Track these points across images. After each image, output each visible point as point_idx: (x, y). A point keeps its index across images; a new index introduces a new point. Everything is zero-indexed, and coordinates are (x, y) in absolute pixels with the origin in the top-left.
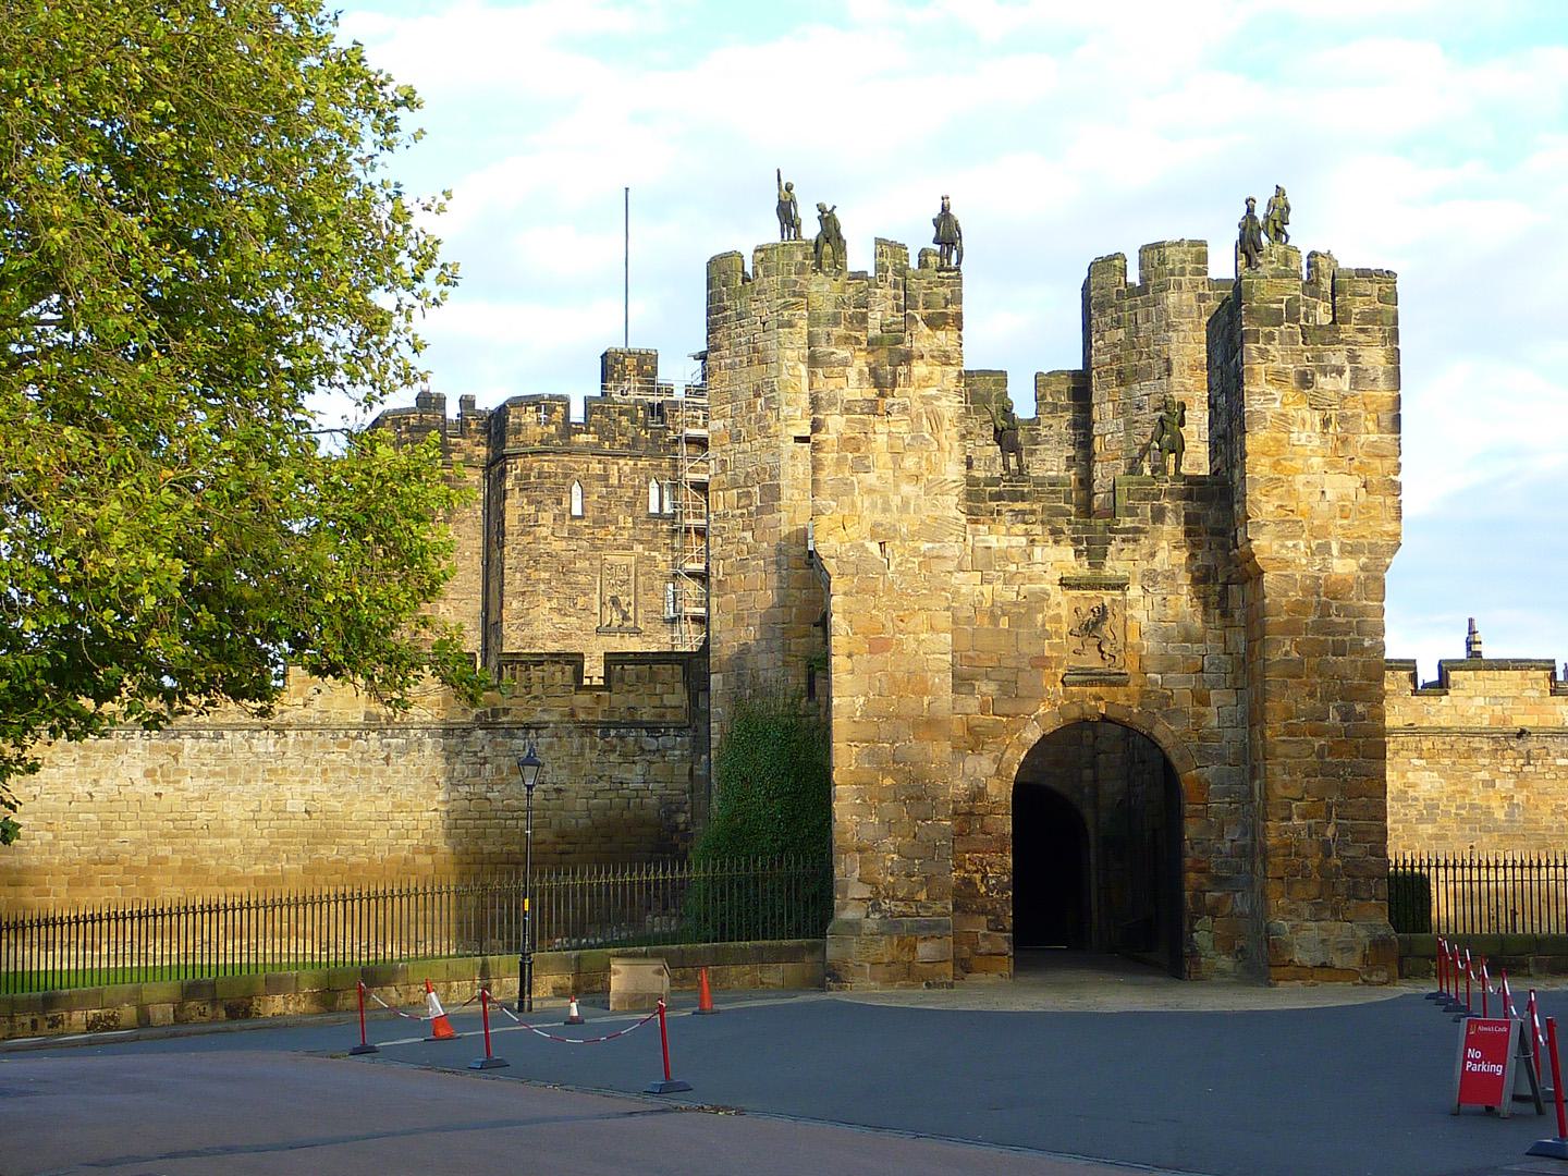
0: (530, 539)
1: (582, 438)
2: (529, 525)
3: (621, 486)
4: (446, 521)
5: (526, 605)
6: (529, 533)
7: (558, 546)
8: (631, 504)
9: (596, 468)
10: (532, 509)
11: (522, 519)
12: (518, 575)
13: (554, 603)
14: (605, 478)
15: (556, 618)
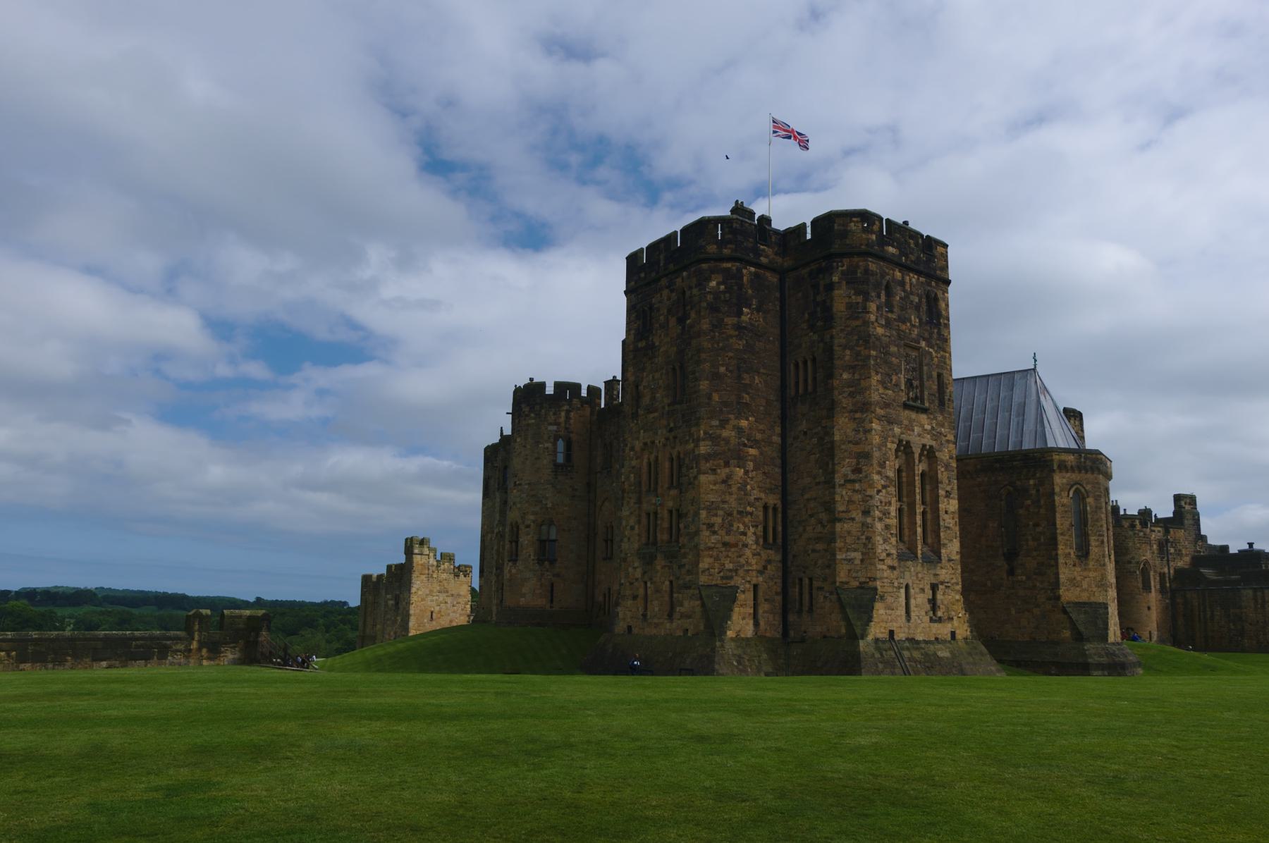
0: (858, 323)
1: (891, 249)
2: (856, 311)
3: (912, 293)
4: (758, 311)
5: (857, 376)
6: (857, 318)
7: (880, 331)
8: (918, 307)
9: (898, 274)
10: (860, 299)
11: (850, 306)
12: (848, 352)
13: (879, 377)
14: (902, 283)
15: (881, 391)
